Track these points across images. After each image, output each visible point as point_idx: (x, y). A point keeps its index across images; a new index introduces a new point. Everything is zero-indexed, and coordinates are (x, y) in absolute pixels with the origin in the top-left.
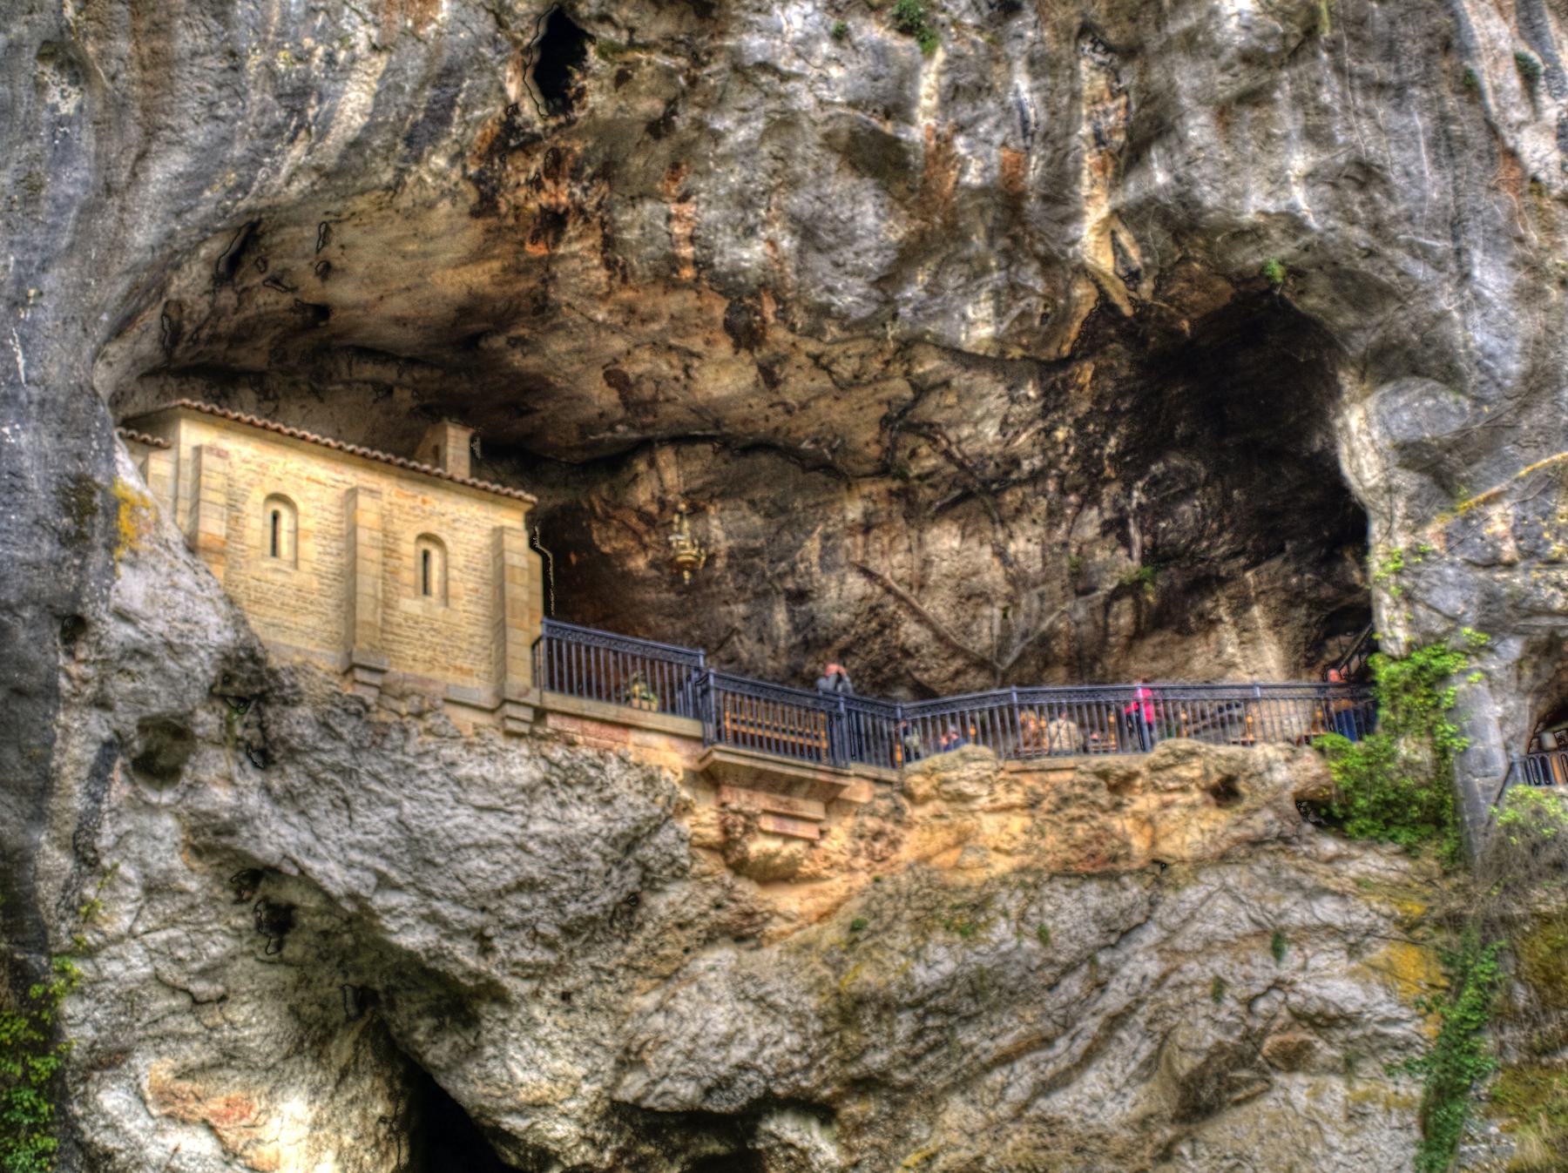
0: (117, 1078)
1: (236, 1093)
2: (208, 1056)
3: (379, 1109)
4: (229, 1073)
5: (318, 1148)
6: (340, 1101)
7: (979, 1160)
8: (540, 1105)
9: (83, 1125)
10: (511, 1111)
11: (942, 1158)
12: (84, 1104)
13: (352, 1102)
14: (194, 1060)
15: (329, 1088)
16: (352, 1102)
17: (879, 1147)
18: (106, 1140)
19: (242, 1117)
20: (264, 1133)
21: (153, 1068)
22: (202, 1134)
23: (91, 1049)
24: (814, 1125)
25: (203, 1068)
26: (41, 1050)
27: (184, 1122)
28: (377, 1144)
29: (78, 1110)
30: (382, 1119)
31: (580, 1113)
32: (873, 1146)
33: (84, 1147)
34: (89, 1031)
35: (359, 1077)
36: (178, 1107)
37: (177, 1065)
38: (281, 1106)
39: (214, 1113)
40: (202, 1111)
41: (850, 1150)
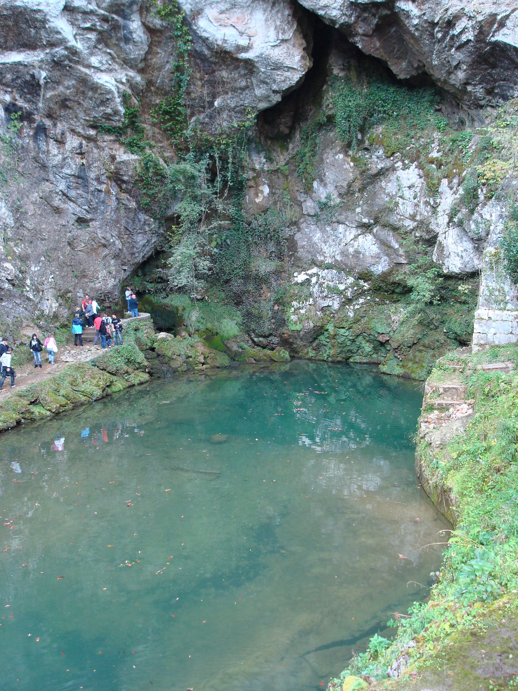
0: (202, 17)
1: (240, 15)
2: (228, 6)
3: (287, 12)
4: (236, 10)
5: (268, 27)
6: (274, 12)
7: (463, 9)
8: (326, 6)
9: (198, 32)
10: (319, 9)
11: (451, 9)
12: (196, 26)
13: (278, 12)
14: (223, 8)
15: (269, 9)
16: (278, 12)
17: (431, 8)
18: (205, 35)
19: (242, 22)
20: (252, 24)
21: (211, 12)
22: (232, 28)
23: (191, 11)
24: (410, 3)
25: (227, 9)
26: (179, 13)
27: (225, 26)
28: (289, 23)
29: (195, 28)
30: (289, 15)
31: (339, 7)
32: (429, 8)
33: (201, 37)
34: (189, 7)
35: (279, 4)
36: (222, 22)
37: (219, 10)
38: (255, 17)
39: (233, 22)
40: (230, 22)
41: (422, 10)
